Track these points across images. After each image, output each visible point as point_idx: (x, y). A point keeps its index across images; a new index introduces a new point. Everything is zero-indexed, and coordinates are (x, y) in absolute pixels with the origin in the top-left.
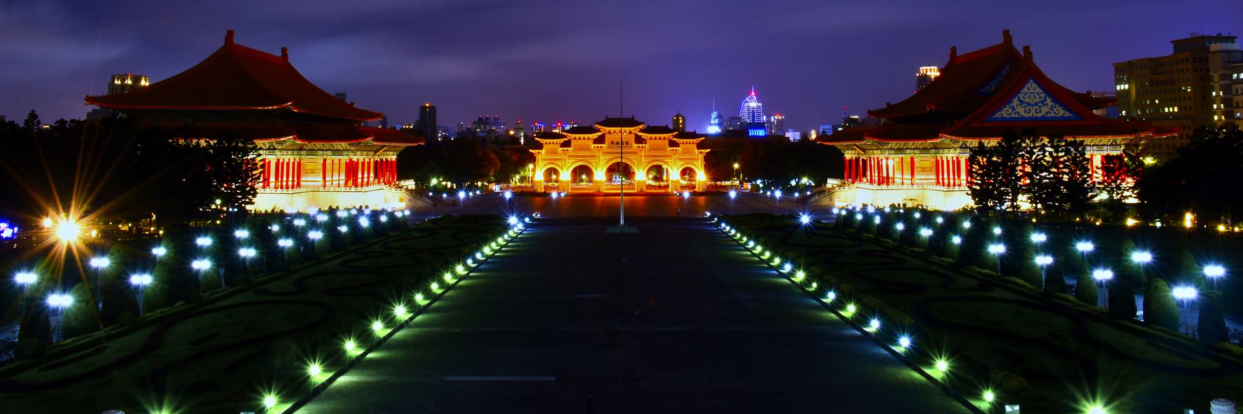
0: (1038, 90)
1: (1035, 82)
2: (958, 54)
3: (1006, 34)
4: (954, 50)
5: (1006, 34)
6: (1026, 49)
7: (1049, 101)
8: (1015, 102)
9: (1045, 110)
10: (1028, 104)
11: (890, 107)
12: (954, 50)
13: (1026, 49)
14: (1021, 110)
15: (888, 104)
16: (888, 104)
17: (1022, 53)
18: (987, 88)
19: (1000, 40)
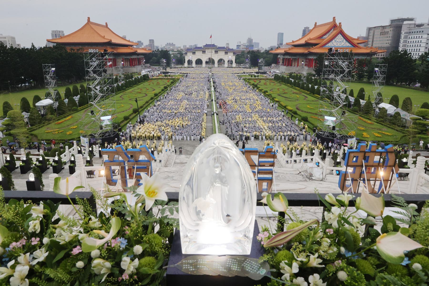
0: (342, 37)
1: (341, 35)
2: (317, 25)
3: (334, 18)
4: (316, 23)
5: (334, 18)
6: (340, 23)
7: (345, 41)
8: (334, 41)
9: (343, 44)
10: (338, 42)
11: (293, 42)
12: (316, 23)
13: (340, 23)
14: (335, 44)
15: (293, 41)
16: (293, 41)
17: (338, 24)
18: (325, 36)
19: (332, 20)
